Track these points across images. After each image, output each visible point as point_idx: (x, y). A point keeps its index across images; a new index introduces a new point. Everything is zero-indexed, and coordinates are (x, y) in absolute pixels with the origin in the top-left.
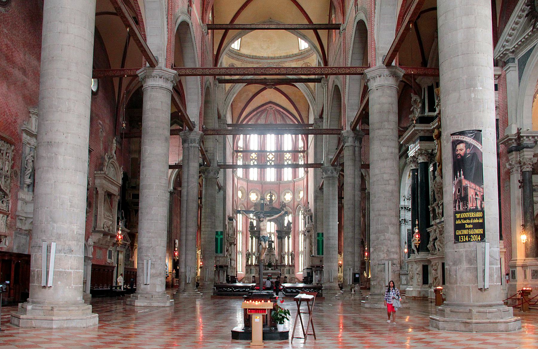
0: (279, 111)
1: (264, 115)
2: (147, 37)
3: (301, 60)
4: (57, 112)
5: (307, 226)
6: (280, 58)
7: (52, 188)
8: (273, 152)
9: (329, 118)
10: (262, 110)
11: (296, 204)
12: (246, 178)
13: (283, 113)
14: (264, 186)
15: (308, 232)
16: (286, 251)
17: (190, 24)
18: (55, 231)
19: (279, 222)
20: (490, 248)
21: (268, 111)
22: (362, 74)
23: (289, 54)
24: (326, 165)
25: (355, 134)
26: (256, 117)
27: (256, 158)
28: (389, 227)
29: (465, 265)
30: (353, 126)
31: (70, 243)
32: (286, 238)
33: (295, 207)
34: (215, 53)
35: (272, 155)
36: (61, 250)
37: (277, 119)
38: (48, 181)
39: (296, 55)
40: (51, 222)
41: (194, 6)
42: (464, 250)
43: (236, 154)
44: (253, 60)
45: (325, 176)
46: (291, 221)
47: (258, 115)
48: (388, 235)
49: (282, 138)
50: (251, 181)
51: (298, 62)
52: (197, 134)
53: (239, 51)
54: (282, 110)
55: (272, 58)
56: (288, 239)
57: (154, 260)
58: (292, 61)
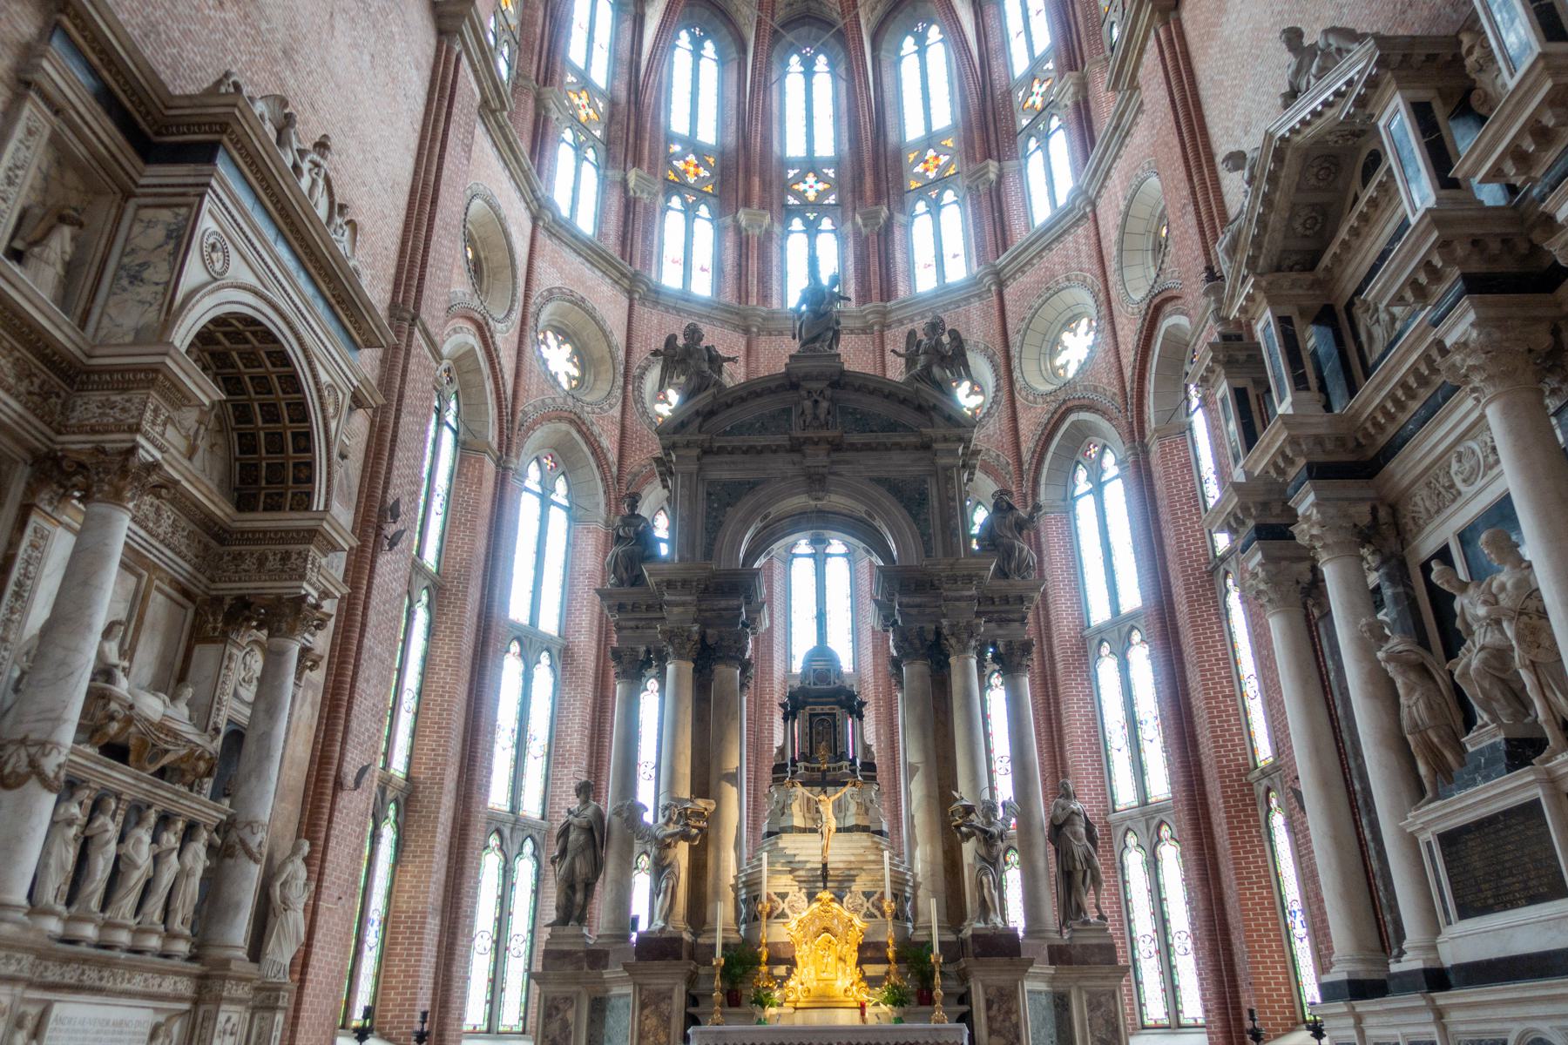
8: (828, 163)
27: (709, 189)
33: (1026, 456)
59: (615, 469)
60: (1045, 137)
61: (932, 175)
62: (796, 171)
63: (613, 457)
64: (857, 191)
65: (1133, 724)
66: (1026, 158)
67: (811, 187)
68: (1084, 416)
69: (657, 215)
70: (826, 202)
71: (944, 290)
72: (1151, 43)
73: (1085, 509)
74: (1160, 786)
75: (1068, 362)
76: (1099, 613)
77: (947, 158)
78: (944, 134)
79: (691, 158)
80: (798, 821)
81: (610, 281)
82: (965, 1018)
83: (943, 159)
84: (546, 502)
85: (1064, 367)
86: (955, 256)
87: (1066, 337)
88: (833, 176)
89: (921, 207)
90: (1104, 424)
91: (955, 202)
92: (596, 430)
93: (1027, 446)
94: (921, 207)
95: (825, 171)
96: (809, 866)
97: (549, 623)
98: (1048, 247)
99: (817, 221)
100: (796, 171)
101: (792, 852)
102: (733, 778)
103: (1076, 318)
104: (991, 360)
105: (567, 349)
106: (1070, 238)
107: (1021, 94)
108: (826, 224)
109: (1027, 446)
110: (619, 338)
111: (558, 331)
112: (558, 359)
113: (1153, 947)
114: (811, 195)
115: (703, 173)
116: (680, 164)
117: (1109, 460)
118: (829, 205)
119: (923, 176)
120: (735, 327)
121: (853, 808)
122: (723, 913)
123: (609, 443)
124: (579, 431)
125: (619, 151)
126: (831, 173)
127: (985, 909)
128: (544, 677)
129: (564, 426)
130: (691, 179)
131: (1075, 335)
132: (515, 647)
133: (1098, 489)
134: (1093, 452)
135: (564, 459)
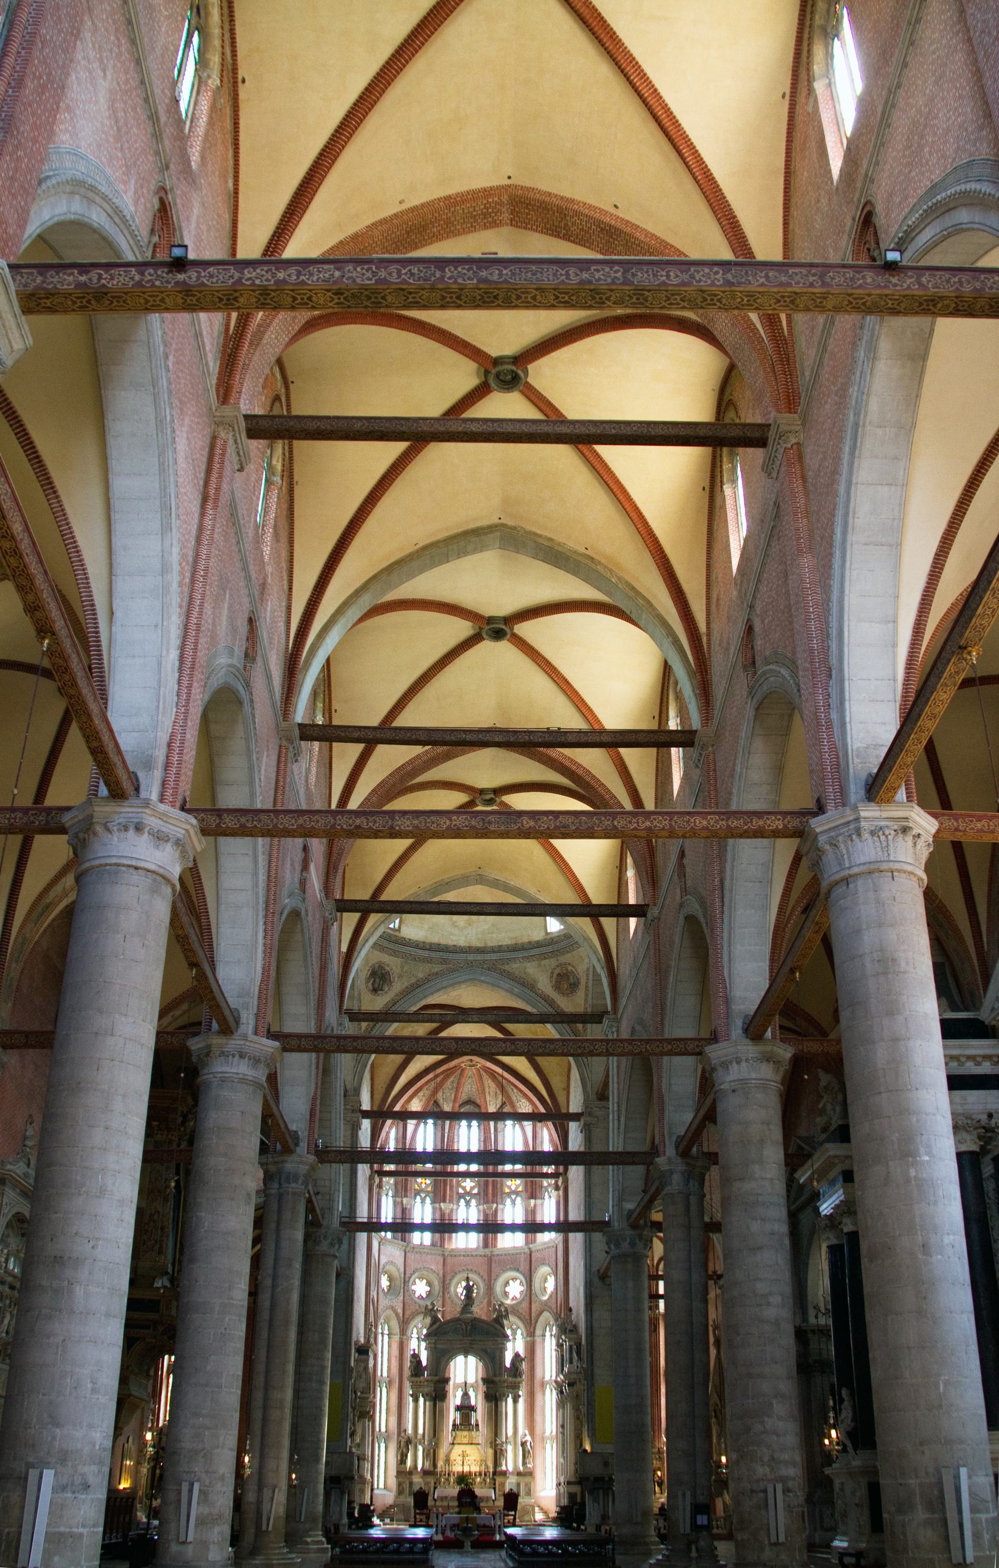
0: (492, 1075)
1: (452, 1079)
2: (217, 964)
3: (550, 958)
4: (79, 1195)
5: (566, 1369)
6: (499, 949)
7: (57, 1353)
9: (623, 1112)
10: (449, 1069)
13: (502, 1076)
14: (449, 1260)
15: (569, 1385)
16: (510, 1432)
17: (303, 912)
18: (57, 1444)
19: (491, 1357)
20: (970, 1477)
21: (463, 1070)
22: (700, 1054)
23: (520, 941)
24: (616, 1224)
25: (688, 1164)
26: (433, 1084)
27: (429, 1189)
28: (771, 1404)
29: (921, 1514)
30: (682, 1146)
31: (86, 1469)
32: (510, 1400)
33: (533, 1315)
34: (344, 948)
36: (67, 1485)
37: (487, 1090)
38: (49, 1338)
39: (538, 945)
40: (49, 1426)
41: (312, 867)
42: (918, 1481)
43: (377, 1180)
44: (433, 954)
45: (614, 1251)
46: (522, 1354)
47: (439, 1079)
48: (770, 1423)
49: (500, 1138)
51: (543, 962)
52: (301, 1162)
53: (396, 934)
54: (499, 1070)
55: (479, 951)
56: (515, 1401)
57: (207, 1482)
58: (527, 958)
61: (513, 1187)
64: (486, 1194)
94: (508, 1201)
104: (526, 1278)
108: (473, 1202)
110: (402, 1270)
112: (385, 1282)
119: (509, 1187)
122: (440, 1463)
125: (400, 1187)
127: (501, 1465)
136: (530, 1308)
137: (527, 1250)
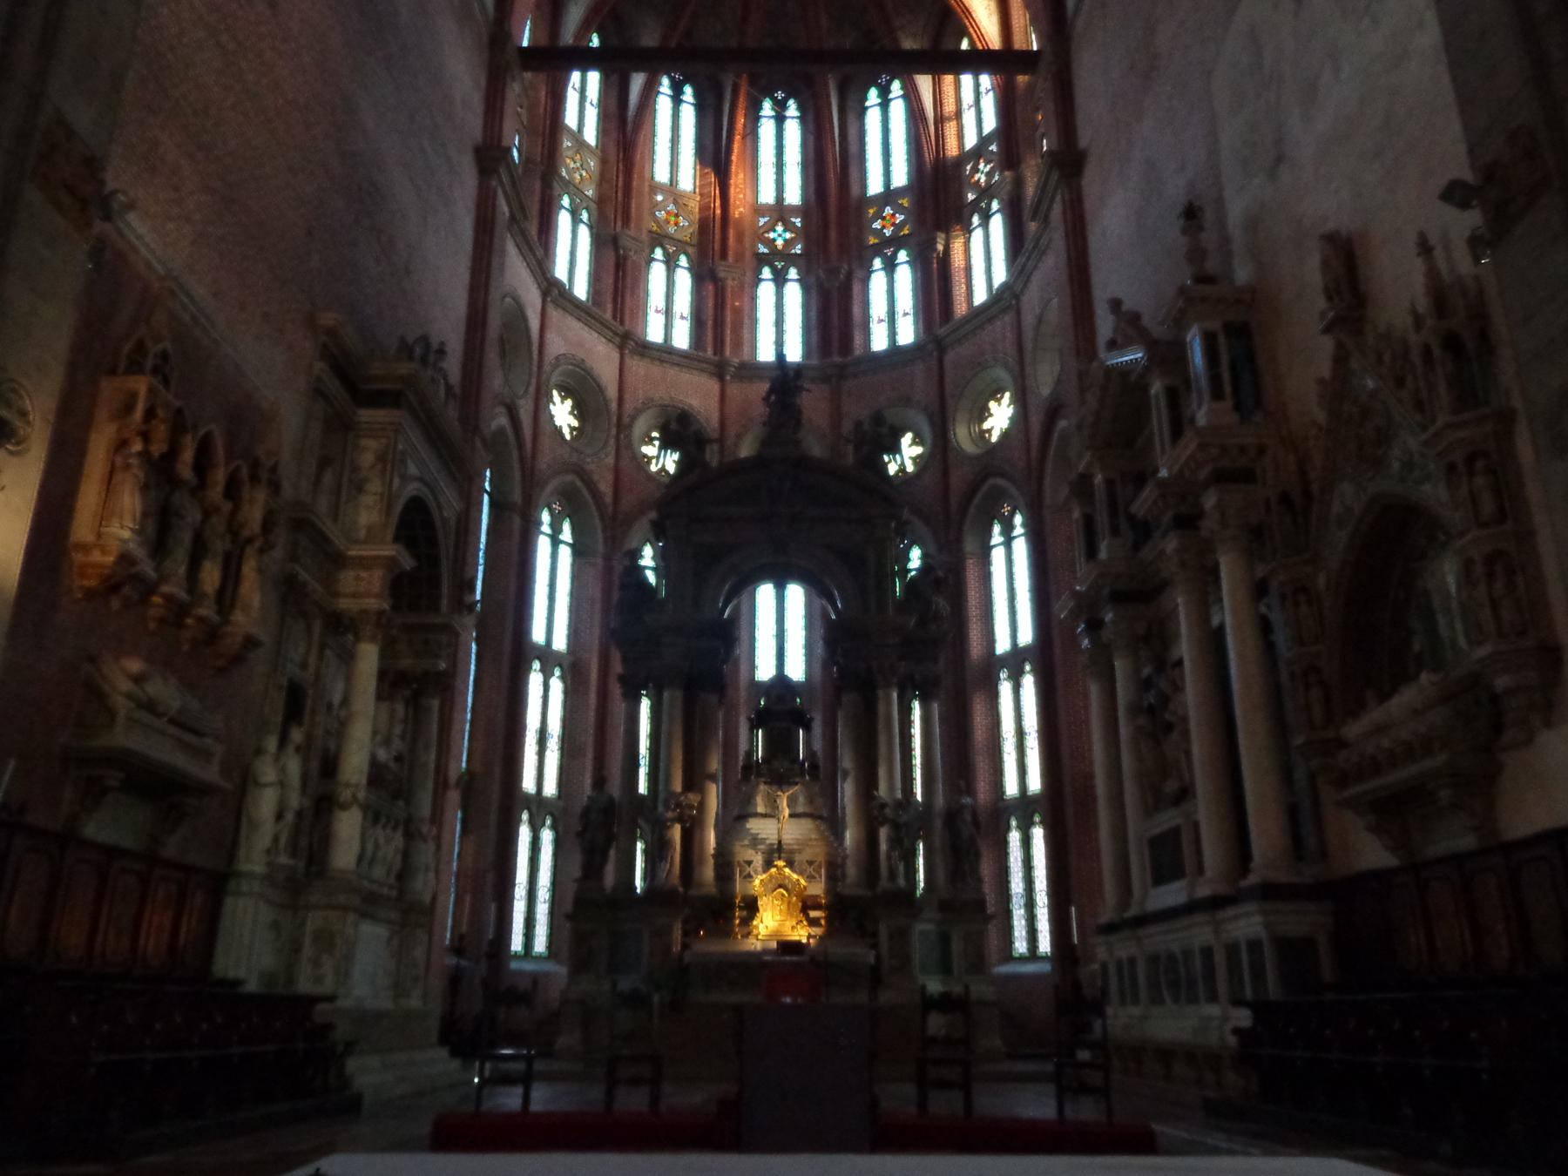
11: (957, 480)
12: (618, 313)
35: (788, 227)
50: (646, 350)
59: (610, 509)
60: (986, 217)
62: (766, 219)
63: (608, 499)
65: (1020, 734)
66: (970, 232)
67: (780, 235)
68: (1000, 482)
69: (643, 269)
70: (793, 251)
71: (895, 350)
72: (1058, 198)
73: (998, 555)
74: (1035, 784)
75: (992, 428)
76: (1002, 646)
77: (902, 217)
78: (900, 192)
79: (671, 207)
80: (760, 809)
81: (604, 340)
82: (875, 946)
83: (900, 218)
84: (555, 542)
85: (989, 431)
86: (906, 314)
87: (992, 405)
88: (799, 225)
89: (877, 263)
90: (1013, 491)
91: (907, 262)
92: (596, 477)
93: (954, 500)
94: (877, 263)
95: (793, 220)
96: (768, 842)
97: (560, 643)
98: (981, 326)
99: (785, 270)
100: (766, 219)
101: (757, 832)
102: (713, 778)
103: (1002, 391)
104: (930, 418)
105: (569, 402)
106: (999, 323)
107: (968, 167)
109: (954, 500)
111: (561, 388)
112: (562, 413)
113: (1022, 902)
114: (780, 243)
115: (682, 222)
116: (661, 215)
117: (1018, 519)
118: (796, 254)
119: (879, 233)
120: (712, 374)
121: (801, 799)
122: (708, 872)
123: (605, 487)
124: (583, 480)
126: (798, 222)
128: (557, 686)
129: (570, 477)
130: (672, 229)
131: (999, 405)
132: (536, 665)
133: (1008, 544)
134: (1006, 510)
135: (572, 506)
136: (946, 488)
137: (930, 347)
